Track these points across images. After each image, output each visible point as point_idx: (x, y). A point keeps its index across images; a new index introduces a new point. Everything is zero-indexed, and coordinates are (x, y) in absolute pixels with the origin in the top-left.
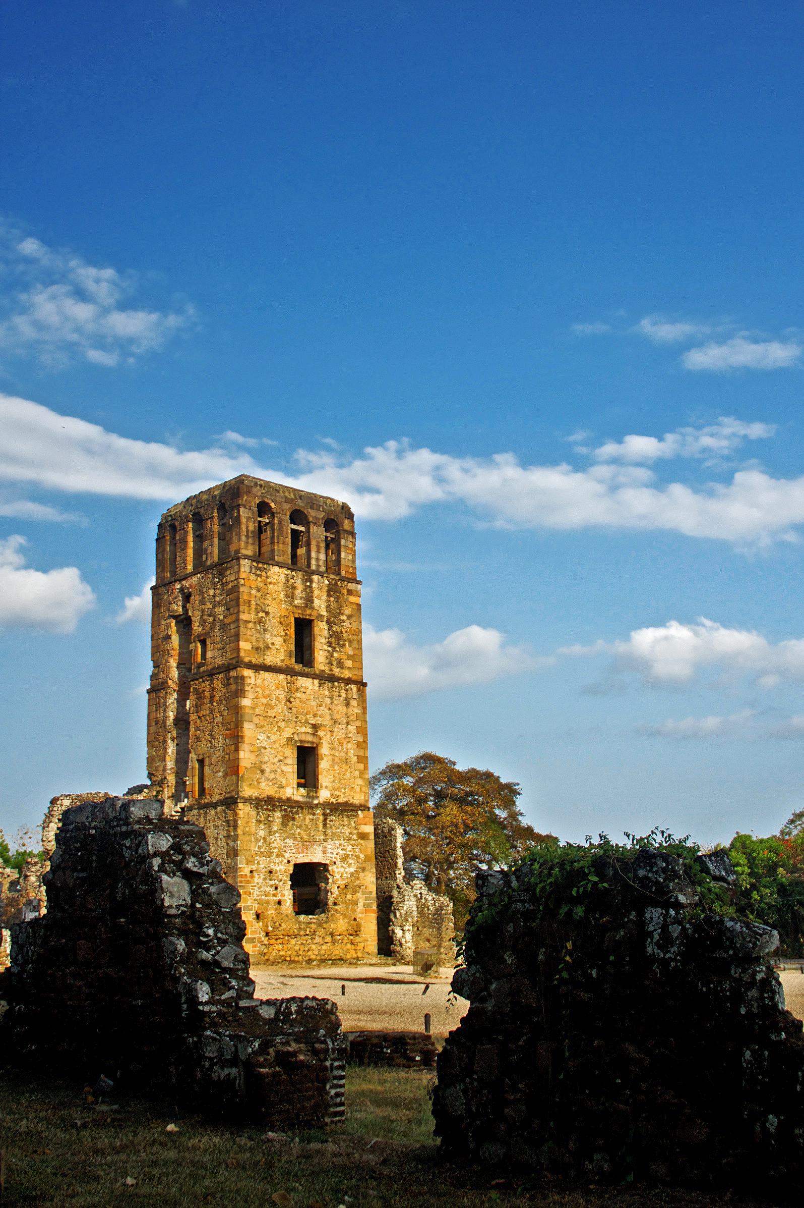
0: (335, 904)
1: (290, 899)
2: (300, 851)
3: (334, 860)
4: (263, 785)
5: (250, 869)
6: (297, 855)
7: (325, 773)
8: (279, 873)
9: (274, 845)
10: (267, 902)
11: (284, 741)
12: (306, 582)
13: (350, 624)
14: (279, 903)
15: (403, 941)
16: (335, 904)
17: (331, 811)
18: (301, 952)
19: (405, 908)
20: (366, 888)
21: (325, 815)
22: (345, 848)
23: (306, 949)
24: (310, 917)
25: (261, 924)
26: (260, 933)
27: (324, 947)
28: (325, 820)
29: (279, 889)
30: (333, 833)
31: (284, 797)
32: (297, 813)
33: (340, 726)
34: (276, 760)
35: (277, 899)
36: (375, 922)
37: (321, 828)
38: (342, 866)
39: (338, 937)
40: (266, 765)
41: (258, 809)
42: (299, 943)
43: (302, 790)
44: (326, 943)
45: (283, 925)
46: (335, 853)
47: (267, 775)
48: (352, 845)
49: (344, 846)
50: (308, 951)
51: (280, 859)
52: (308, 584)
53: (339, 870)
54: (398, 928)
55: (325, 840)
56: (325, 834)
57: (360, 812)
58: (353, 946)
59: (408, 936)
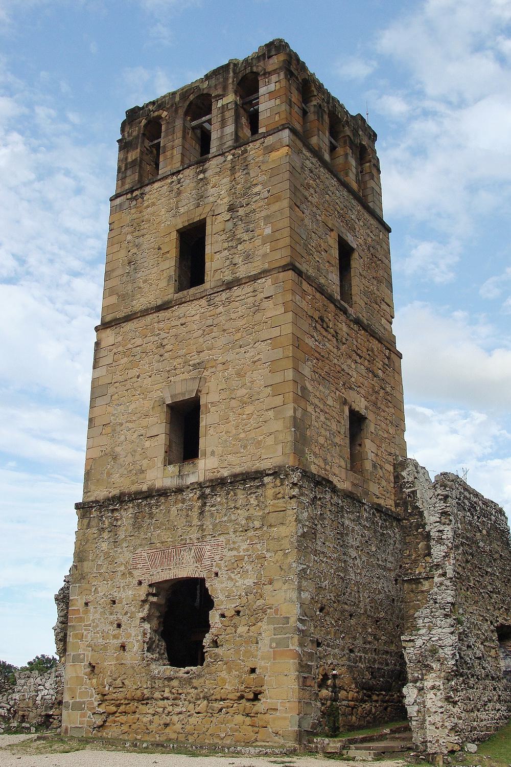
0: (215, 644)
1: (138, 641)
2: (158, 562)
3: (215, 569)
4: (116, 477)
5: (84, 601)
6: (153, 571)
7: (211, 431)
8: (124, 603)
9: (121, 559)
10: (105, 648)
11: (148, 404)
12: (198, 174)
13: (269, 191)
14: (123, 647)
15: (412, 711)
16: (215, 644)
17: (213, 488)
18: (152, 727)
19: (419, 642)
20: (276, 611)
21: (203, 497)
22: (236, 546)
23: (162, 722)
24: (187, 668)
25: (94, 681)
26: (92, 696)
27: (193, 720)
28: (204, 504)
29: (123, 627)
30: (215, 525)
31: (145, 488)
32: (158, 506)
33: (243, 350)
34: (135, 435)
35: (120, 641)
36: (293, 674)
37: (196, 522)
38: (230, 578)
39: (222, 703)
40: (120, 448)
41: (101, 512)
42: (151, 711)
43: (171, 469)
44: (198, 713)
45: (126, 682)
46: (217, 558)
47: (122, 460)
48: (251, 538)
49: (234, 542)
50: (166, 725)
51: (127, 581)
52: (201, 176)
53: (224, 585)
54: (411, 684)
55: (201, 539)
56: (201, 528)
57: (266, 480)
58: (248, 718)
59: (433, 700)
